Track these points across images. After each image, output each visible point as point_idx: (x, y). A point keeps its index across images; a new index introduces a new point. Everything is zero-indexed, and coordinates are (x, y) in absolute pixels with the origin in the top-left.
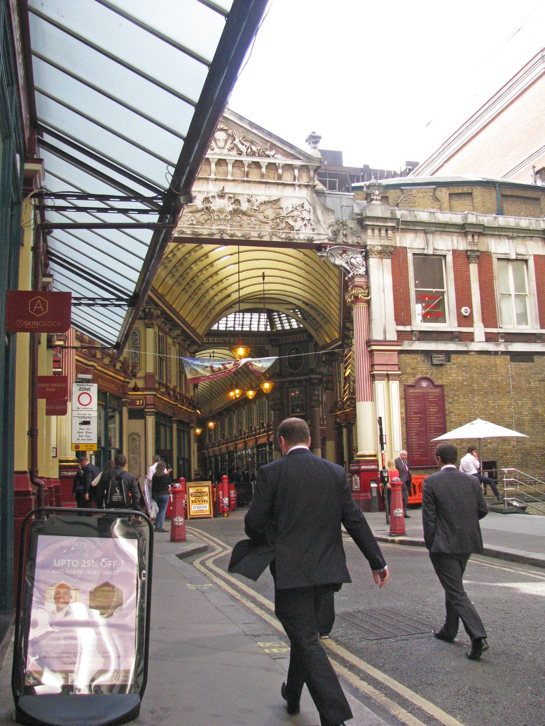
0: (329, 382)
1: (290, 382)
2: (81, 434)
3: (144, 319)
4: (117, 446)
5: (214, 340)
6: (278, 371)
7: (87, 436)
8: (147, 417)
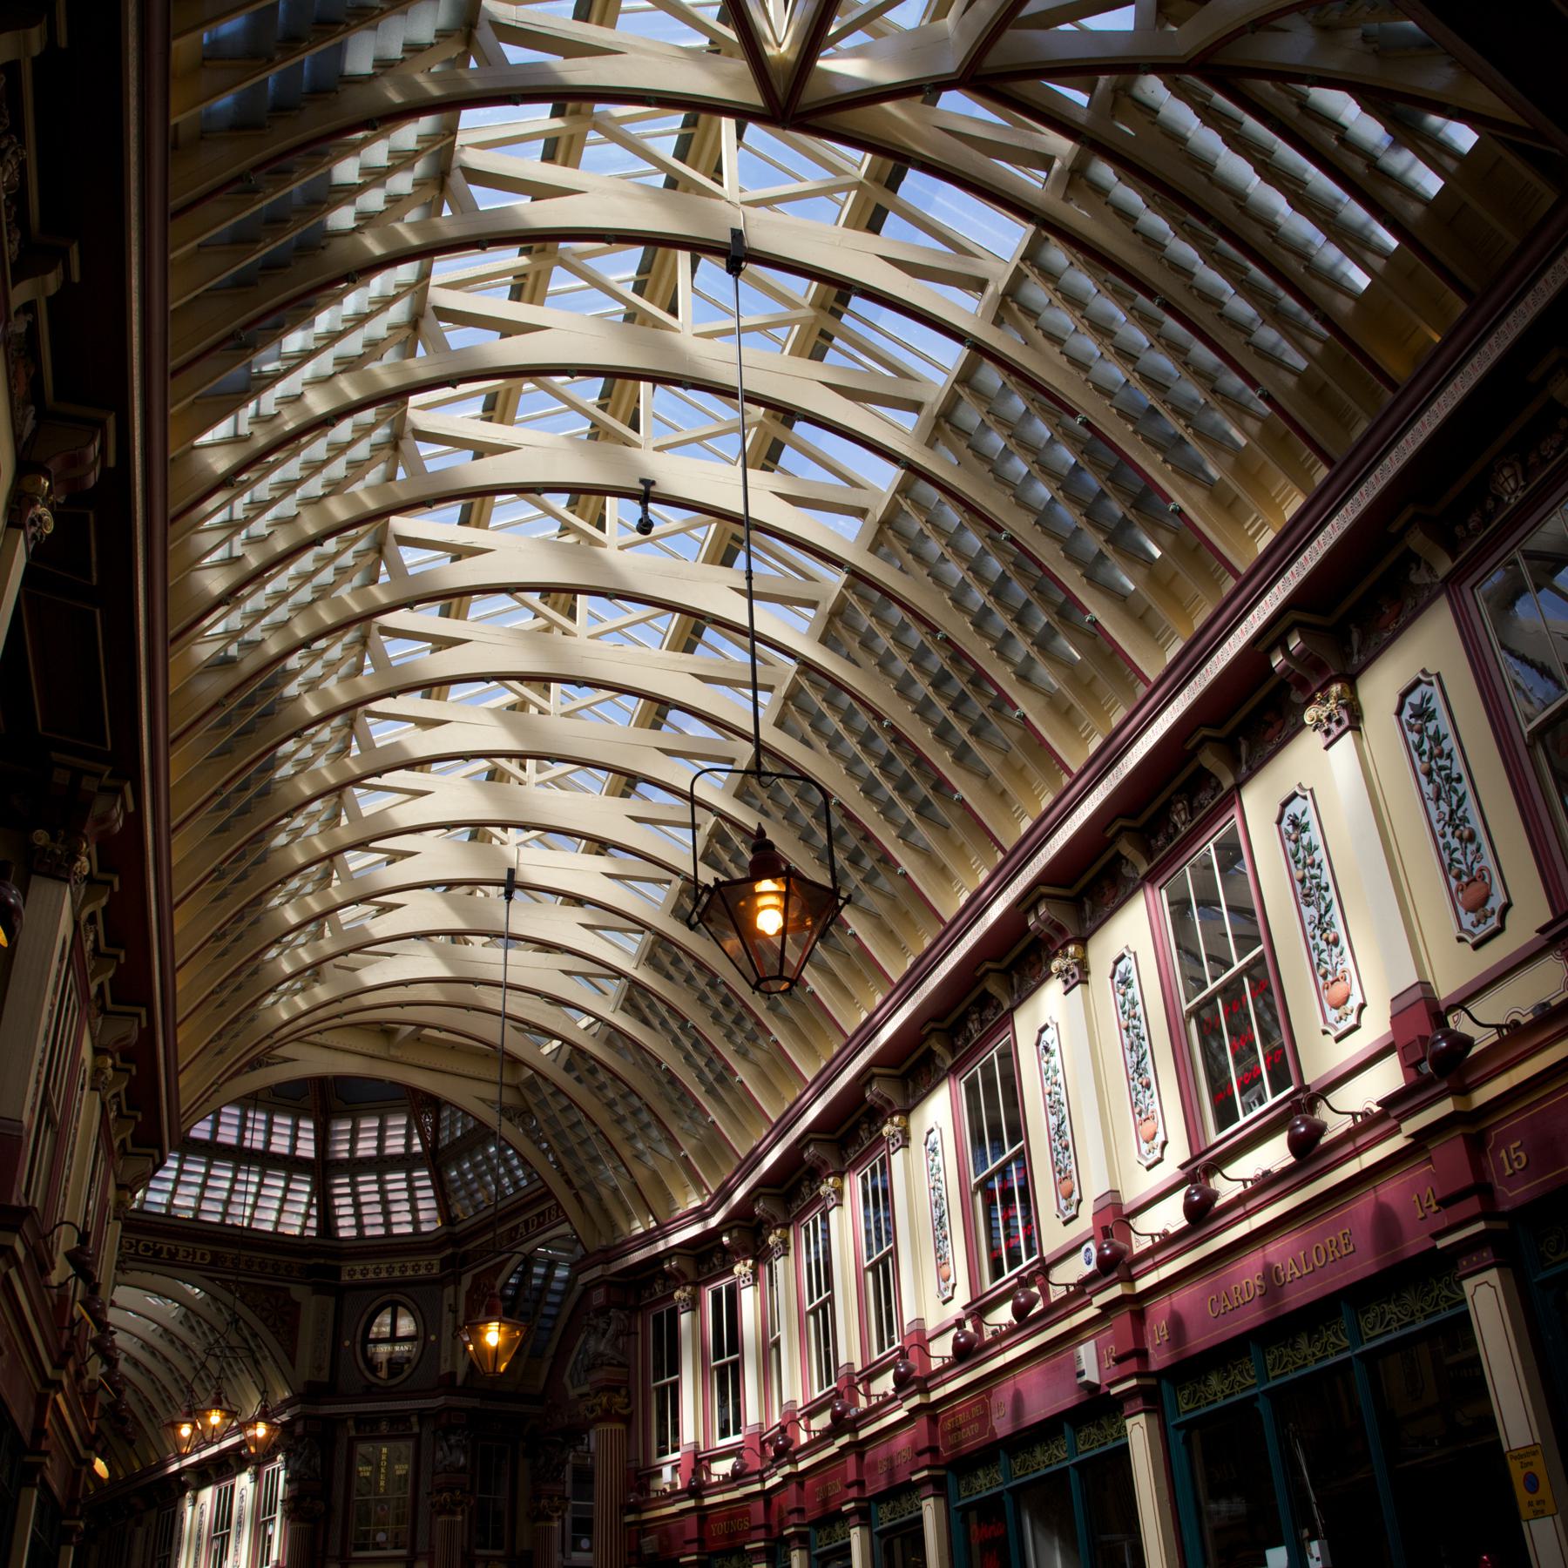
1: (361, 1420)
6: (326, 1379)
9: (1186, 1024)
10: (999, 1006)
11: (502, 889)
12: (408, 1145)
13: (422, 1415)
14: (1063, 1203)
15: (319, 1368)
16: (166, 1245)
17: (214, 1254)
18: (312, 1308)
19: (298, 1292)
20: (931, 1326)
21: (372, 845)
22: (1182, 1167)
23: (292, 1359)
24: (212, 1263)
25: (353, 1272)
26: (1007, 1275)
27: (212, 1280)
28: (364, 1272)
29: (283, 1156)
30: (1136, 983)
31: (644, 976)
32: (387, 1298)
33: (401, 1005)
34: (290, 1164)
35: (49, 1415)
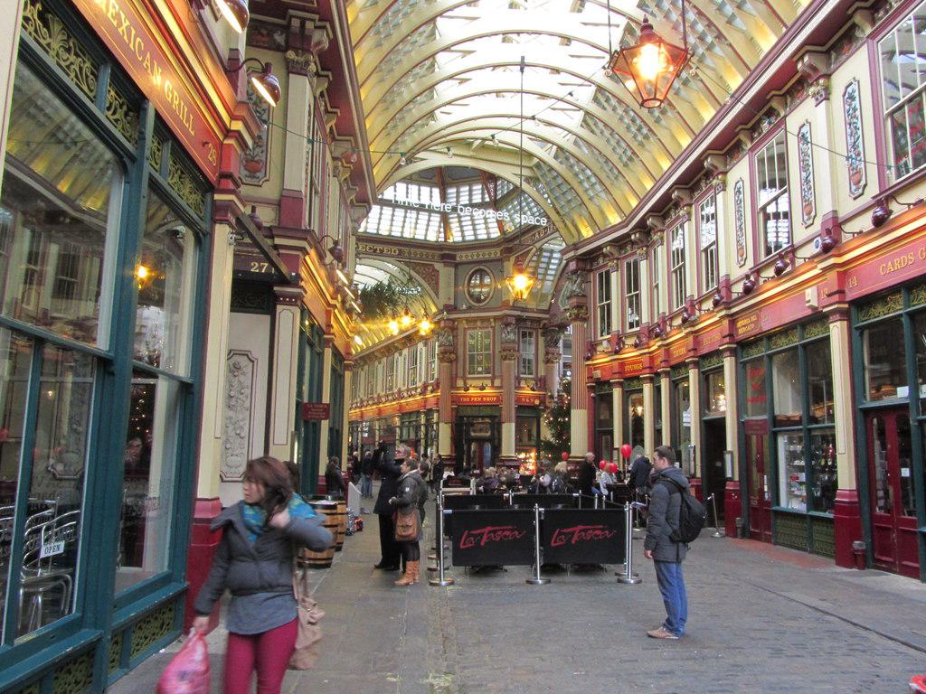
9: (885, 120)
10: (779, 114)
11: (519, 67)
12: (483, 198)
13: (496, 318)
14: (806, 217)
15: (449, 299)
16: (379, 247)
17: (400, 251)
18: (445, 273)
19: (438, 266)
20: (733, 278)
21: (452, 48)
22: (874, 198)
23: (437, 294)
25: (462, 256)
26: (774, 253)
27: (400, 261)
28: (467, 256)
30: (857, 99)
31: (593, 108)
32: (477, 268)
33: (474, 130)
35: (332, 318)
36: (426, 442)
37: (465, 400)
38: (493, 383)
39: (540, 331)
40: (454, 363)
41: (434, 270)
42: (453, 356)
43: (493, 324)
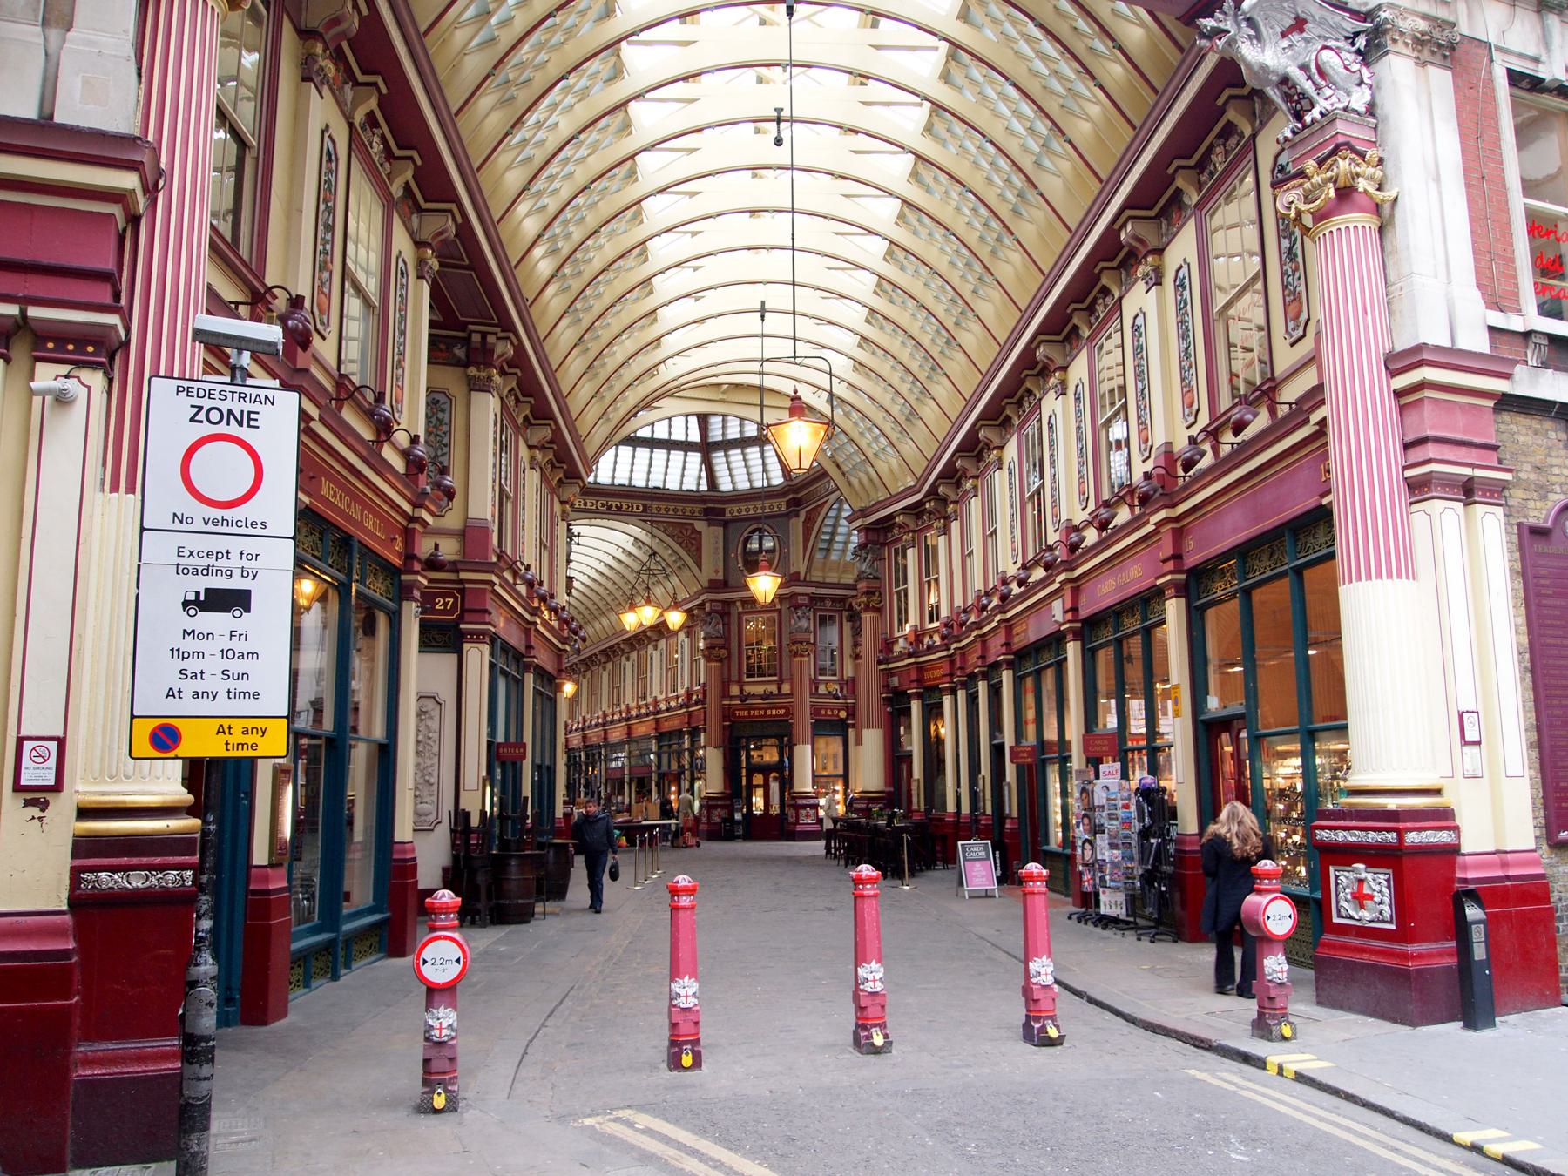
0: (873, 593)
2: (193, 665)
3: (466, 365)
4: (379, 733)
5: (585, 504)
7: (226, 675)
8: (466, 646)
15: (717, 572)
16: (615, 502)
17: (644, 506)
18: (711, 536)
19: (700, 526)
24: (645, 510)
25: (733, 510)
28: (747, 510)
29: (682, 442)
32: (755, 526)
34: (686, 446)
36: (692, 774)
37: (742, 713)
38: (779, 689)
39: (845, 614)
40: (726, 662)
41: (695, 531)
42: (724, 652)
43: (778, 607)
